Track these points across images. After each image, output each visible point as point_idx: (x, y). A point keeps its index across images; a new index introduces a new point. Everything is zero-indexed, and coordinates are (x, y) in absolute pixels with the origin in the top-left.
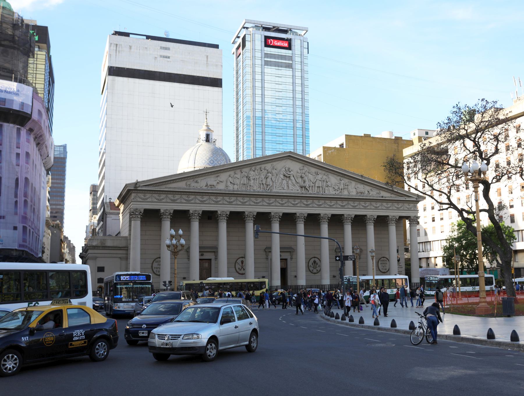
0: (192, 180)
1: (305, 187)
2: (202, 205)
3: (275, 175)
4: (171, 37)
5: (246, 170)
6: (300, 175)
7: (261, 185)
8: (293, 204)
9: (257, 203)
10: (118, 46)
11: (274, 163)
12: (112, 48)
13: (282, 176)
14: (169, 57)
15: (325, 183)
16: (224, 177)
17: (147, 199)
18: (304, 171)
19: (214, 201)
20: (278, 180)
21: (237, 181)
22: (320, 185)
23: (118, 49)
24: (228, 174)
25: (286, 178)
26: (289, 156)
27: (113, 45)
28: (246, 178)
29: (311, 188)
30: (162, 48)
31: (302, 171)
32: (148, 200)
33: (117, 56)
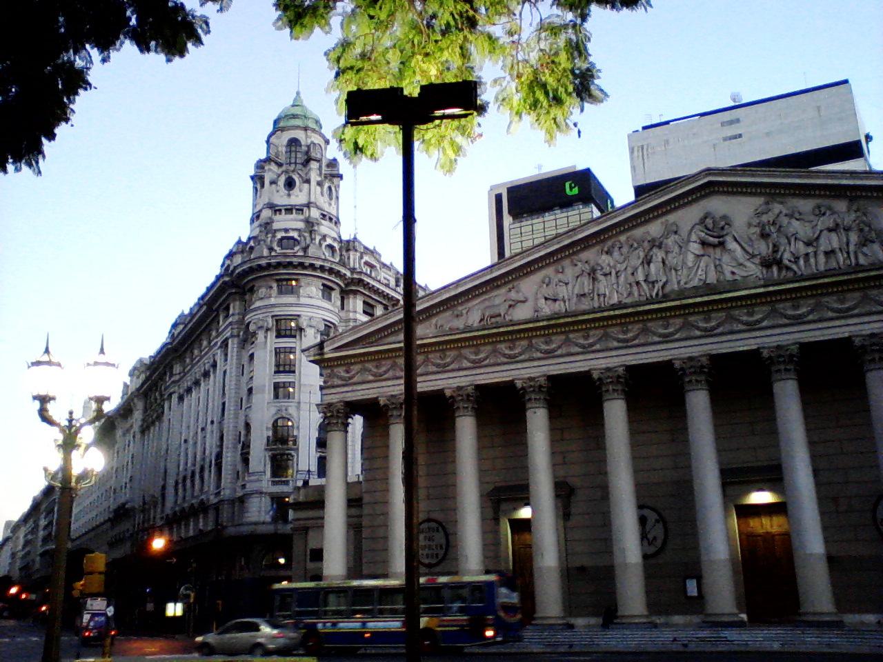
0: (448, 313)
1: (779, 263)
2: (478, 371)
3: (676, 249)
4: (744, 102)
5: (589, 255)
6: (758, 230)
7: (635, 288)
8: (747, 324)
9: (626, 341)
10: (645, 147)
11: (671, 218)
12: (636, 153)
13: (695, 248)
14: (740, 136)
15: (854, 237)
16: (528, 286)
17: (350, 378)
18: (769, 217)
19: (504, 355)
20: (684, 263)
21: (563, 292)
22: (835, 245)
23: (645, 153)
24: (537, 277)
25: (711, 250)
26: (710, 183)
27: (636, 149)
28: (586, 280)
29: (802, 262)
30: (723, 124)
31: (765, 218)
32: (355, 380)
33: (646, 165)
